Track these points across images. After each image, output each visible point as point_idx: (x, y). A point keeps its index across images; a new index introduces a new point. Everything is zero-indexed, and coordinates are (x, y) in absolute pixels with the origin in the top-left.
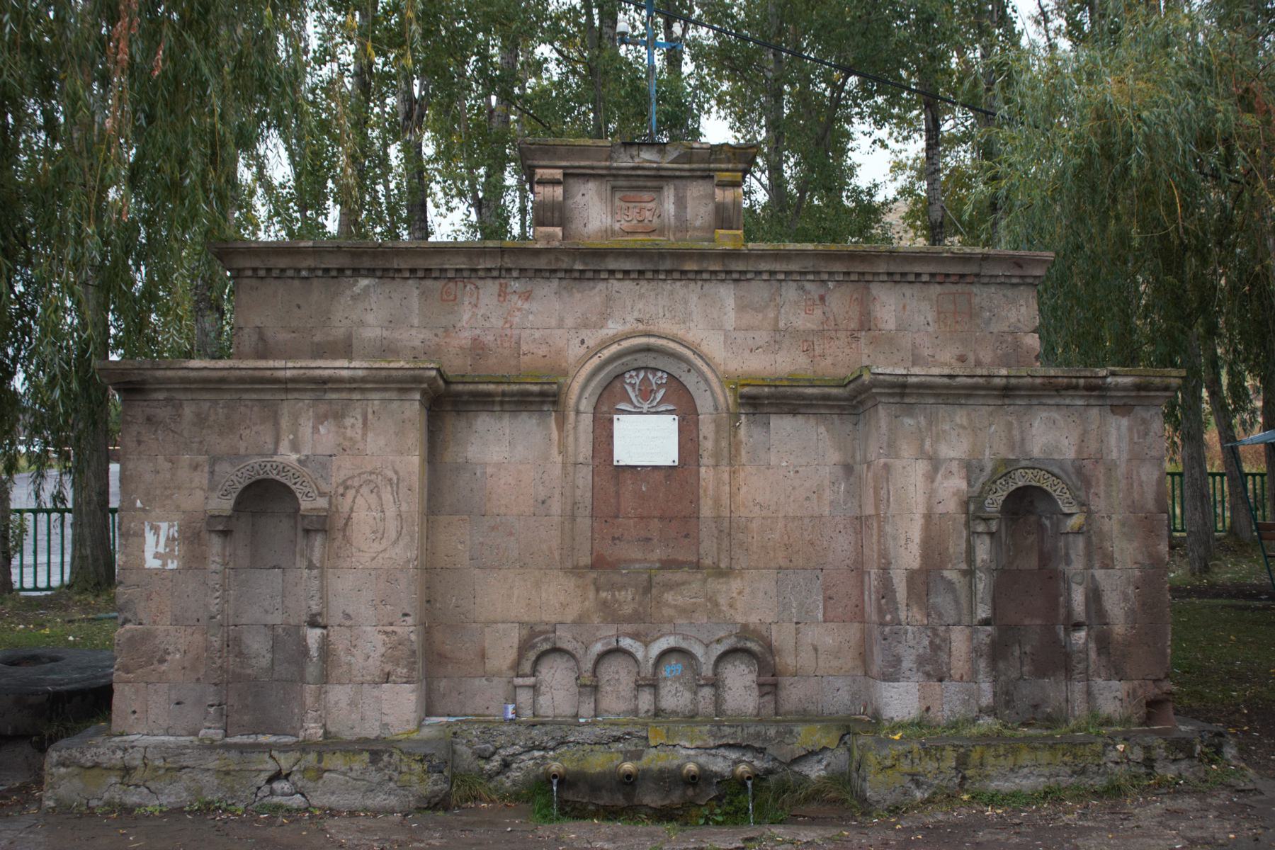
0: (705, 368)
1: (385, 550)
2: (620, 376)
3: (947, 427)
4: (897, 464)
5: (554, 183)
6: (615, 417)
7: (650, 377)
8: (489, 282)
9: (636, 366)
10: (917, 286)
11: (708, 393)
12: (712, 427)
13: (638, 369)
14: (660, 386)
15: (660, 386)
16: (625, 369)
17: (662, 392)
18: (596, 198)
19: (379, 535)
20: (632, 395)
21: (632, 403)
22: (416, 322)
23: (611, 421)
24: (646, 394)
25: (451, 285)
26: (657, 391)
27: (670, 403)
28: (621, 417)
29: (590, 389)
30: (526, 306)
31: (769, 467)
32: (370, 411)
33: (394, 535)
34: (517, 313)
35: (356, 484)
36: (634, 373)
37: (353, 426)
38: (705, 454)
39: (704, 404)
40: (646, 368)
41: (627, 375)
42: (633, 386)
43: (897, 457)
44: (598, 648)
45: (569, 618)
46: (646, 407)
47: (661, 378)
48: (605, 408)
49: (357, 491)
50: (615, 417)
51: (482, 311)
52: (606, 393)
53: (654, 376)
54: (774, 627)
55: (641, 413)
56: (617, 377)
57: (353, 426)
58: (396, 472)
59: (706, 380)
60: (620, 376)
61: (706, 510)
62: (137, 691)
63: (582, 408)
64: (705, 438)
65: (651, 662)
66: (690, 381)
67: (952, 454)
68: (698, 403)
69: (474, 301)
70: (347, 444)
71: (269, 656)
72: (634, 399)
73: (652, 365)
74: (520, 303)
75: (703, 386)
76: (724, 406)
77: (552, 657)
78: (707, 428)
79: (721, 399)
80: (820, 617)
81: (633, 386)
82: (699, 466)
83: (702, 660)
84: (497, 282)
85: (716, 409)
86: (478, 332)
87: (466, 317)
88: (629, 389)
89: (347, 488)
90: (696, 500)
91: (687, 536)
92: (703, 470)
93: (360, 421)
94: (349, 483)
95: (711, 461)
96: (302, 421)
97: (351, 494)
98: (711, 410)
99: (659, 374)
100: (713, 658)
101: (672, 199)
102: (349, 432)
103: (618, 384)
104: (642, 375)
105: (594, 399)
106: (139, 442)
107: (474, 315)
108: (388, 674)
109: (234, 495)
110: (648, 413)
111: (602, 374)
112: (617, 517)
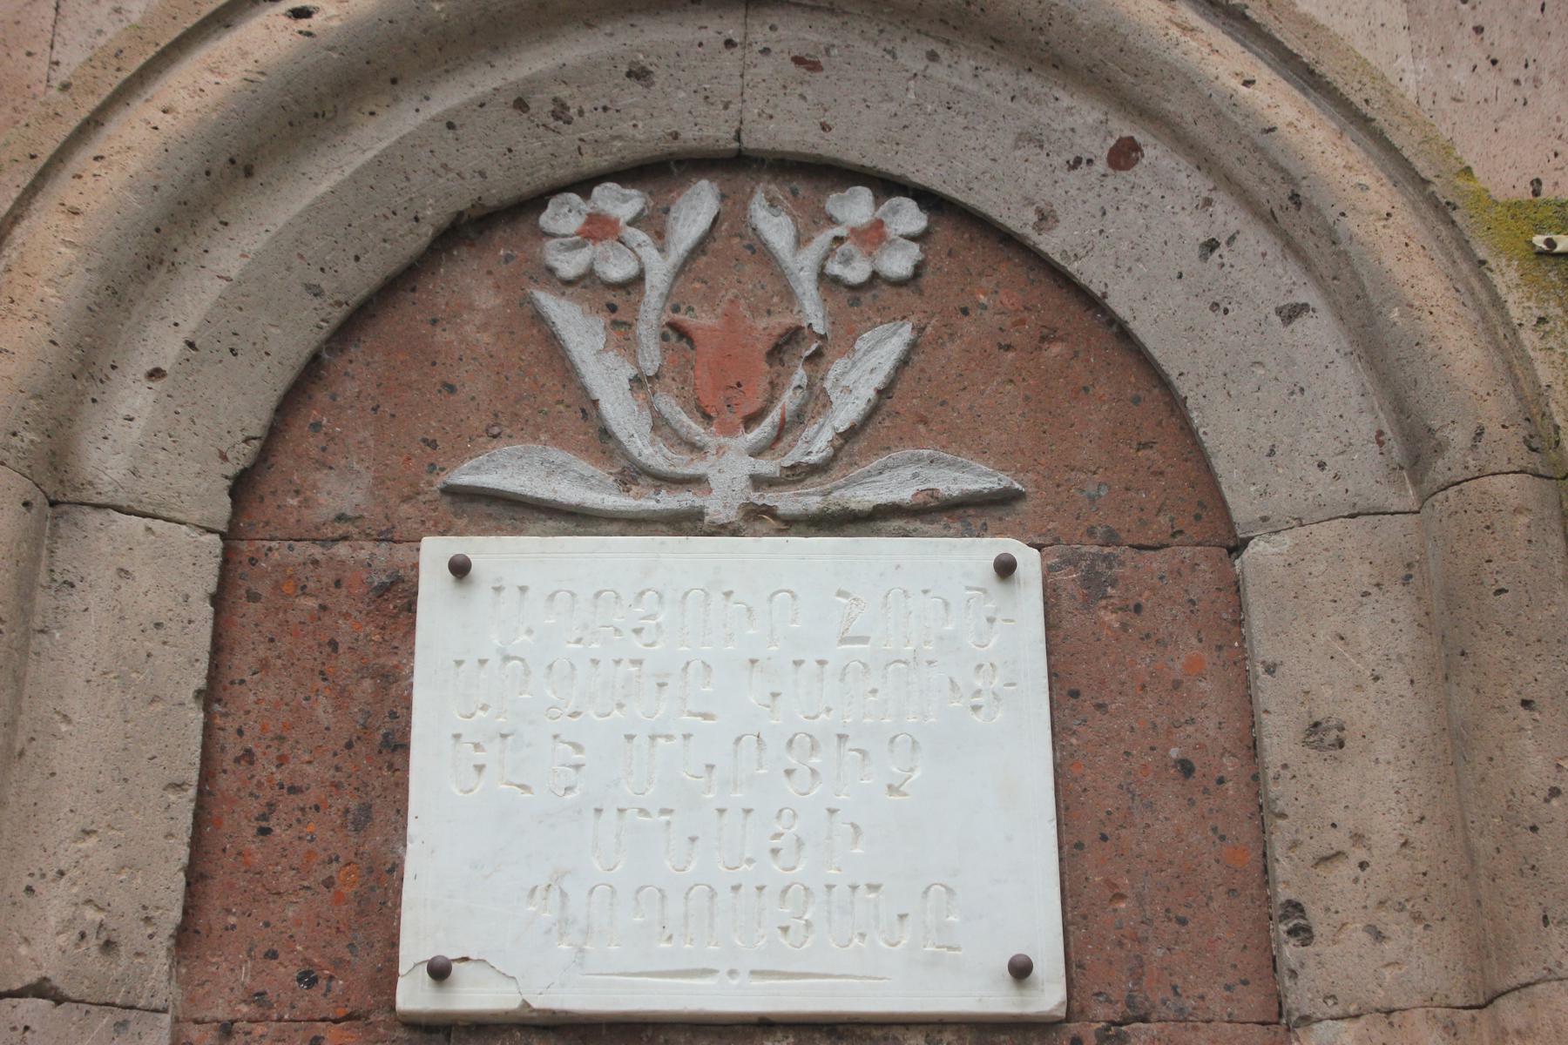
0: (1276, 101)
2: (492, 222)
6: (435, 552)
7: (776, 229)
9: (645, 126)
11: (1321, 331)
12: (1386, 630)
13: (657, 172)
14: (859, 300)
15: (859, 300)
16: (538, 154)
17: (878, 354)
20: (607, 379)
21: (602, 442)
23: (396, 600)
24: (736, 362)
26: (844, 337)
27: (962, 439)
28: (491, 552)
29: (192, 299)
36: (620, 203)
38: (1337, 897)
39: (1282, 420)
40: (734, 164)
41: (564, 217)
46: (730, 469)
47: (873, 236)
48: (340, 492)
50: (435, 552)
52: (358, 372)
53: (813, 220)
55: (686, 523)
56: (469, 229)
59: (1289, 211)
60: (492, 222)
63: (106, 460)
64: (1323, 736)
66: (1139, 243)
68: (1223, 427)
72: (621, 411)
73: (788, 131)
75: (1260, 270)
76: (1495, 410)
78: (1329, 636)
79: (1458, 351)
81: (615, 300)
85: (1415, 449)
88: (564, 314)
95: (1421, 963)
98: (1366, 474)
99: (856, 207)
103: (475, 287)
104: (697, 207)
105: (242, 403)
110: (756, 519)
111: (323, 176)
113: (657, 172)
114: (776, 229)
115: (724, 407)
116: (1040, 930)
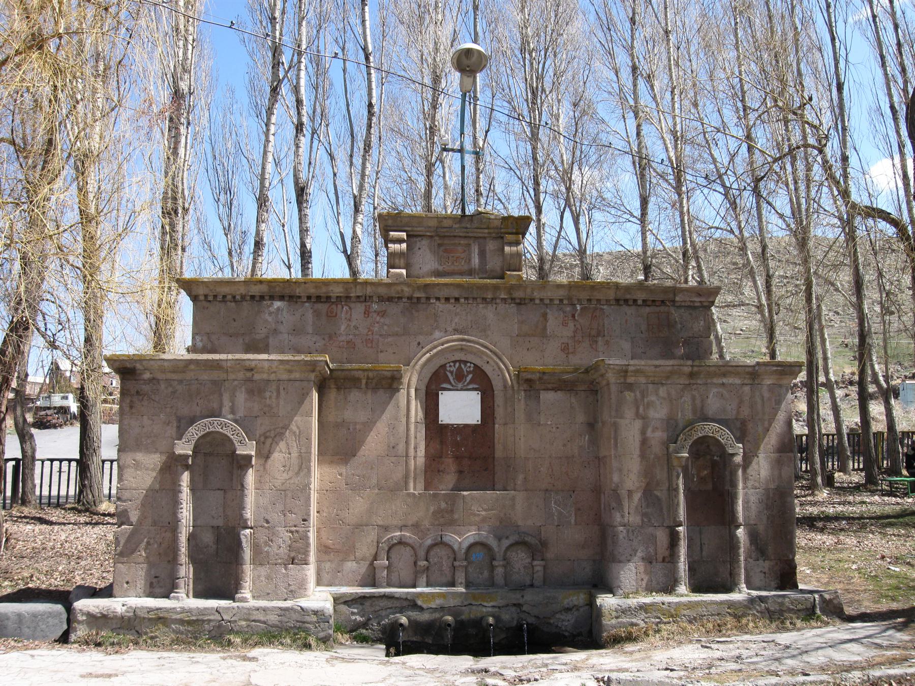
1: (291, 478)
3: (653, 398)
4: (622, 422)
5: (400, 241)
7: (463, 366)
8: (359, 305)
9: (454, 359)
10: (633, 307)
14: (469, 373)
15: (469, 373)
17: (470, 376)
18: (428, 251)
19: (287, 468)
20: (451, 378)
21: (450, 383)
22: (310, 330)
25: (334, 306)
27: (475, 383)
30: (382, 320)
31: (539, 424)
32: (281, 388)
33: (297, 469)
34: (376, 325)
35: (272, 435)
37: (270, 397)
40: (460, 361)
42: (451, 372)
43: (622, 417)
44: (429, 542)
45: (410, 523)
46: (460, 385)
49: (273, 440)
51: (354, 324)
53: (465, 365)
54: (542, 528)
57: (270, 397)
58: (298, 428)
61: (499, 453)
62: (129, 568)
65: (463, 551)
67: (657, 416)
68: (493, 383)
69: (348, 316)
70: (266, 409)
71: (214, 547)
73: (464, 359)
74: (378, 318)
77: (398, 547)
78: (499, 400)
80: (573, 521)
81: (451, 372)
82: (494, 424)
83: (496, 549)
84: (364, 304)
86: (351, 337)
87: (343, 328)
88: (449, 374)
89: (266, 438)
90: (492, 447)
91: (486, 470)
92: (497, 426)
93: (275, 394)
94: (268, 434)
96: (238, 394)
97: (269, 441)
98: (502, 388)
100: (504, 549)
101: (477, 251)
102: (268, 401)
106: (131, 407)
107: (348, 326)
108: (293, 559)
109: (193, 442)
110: (461, 390)
112: (441, 457)
113: (455, 362)
114: (463, 366)
115: (460, 381)
116: (479, 418)
